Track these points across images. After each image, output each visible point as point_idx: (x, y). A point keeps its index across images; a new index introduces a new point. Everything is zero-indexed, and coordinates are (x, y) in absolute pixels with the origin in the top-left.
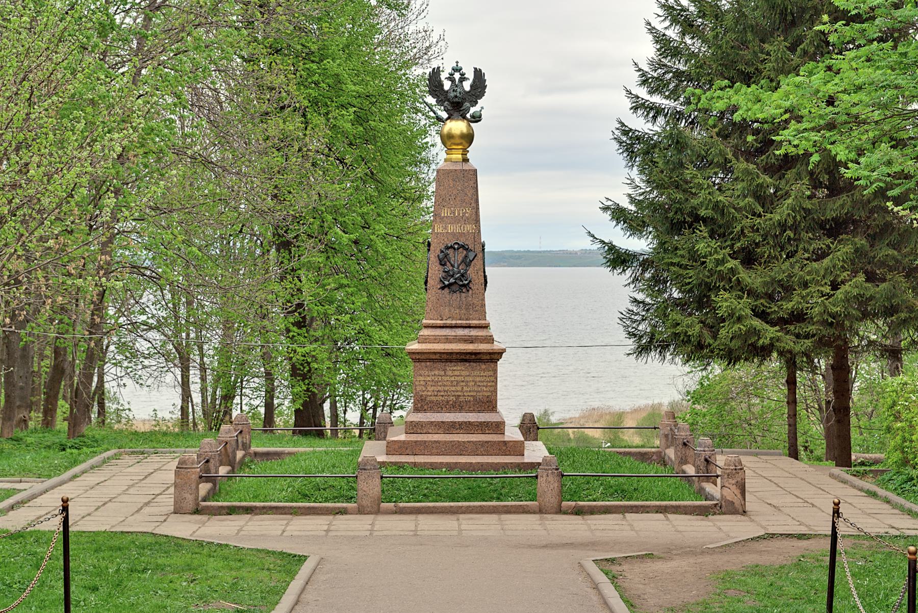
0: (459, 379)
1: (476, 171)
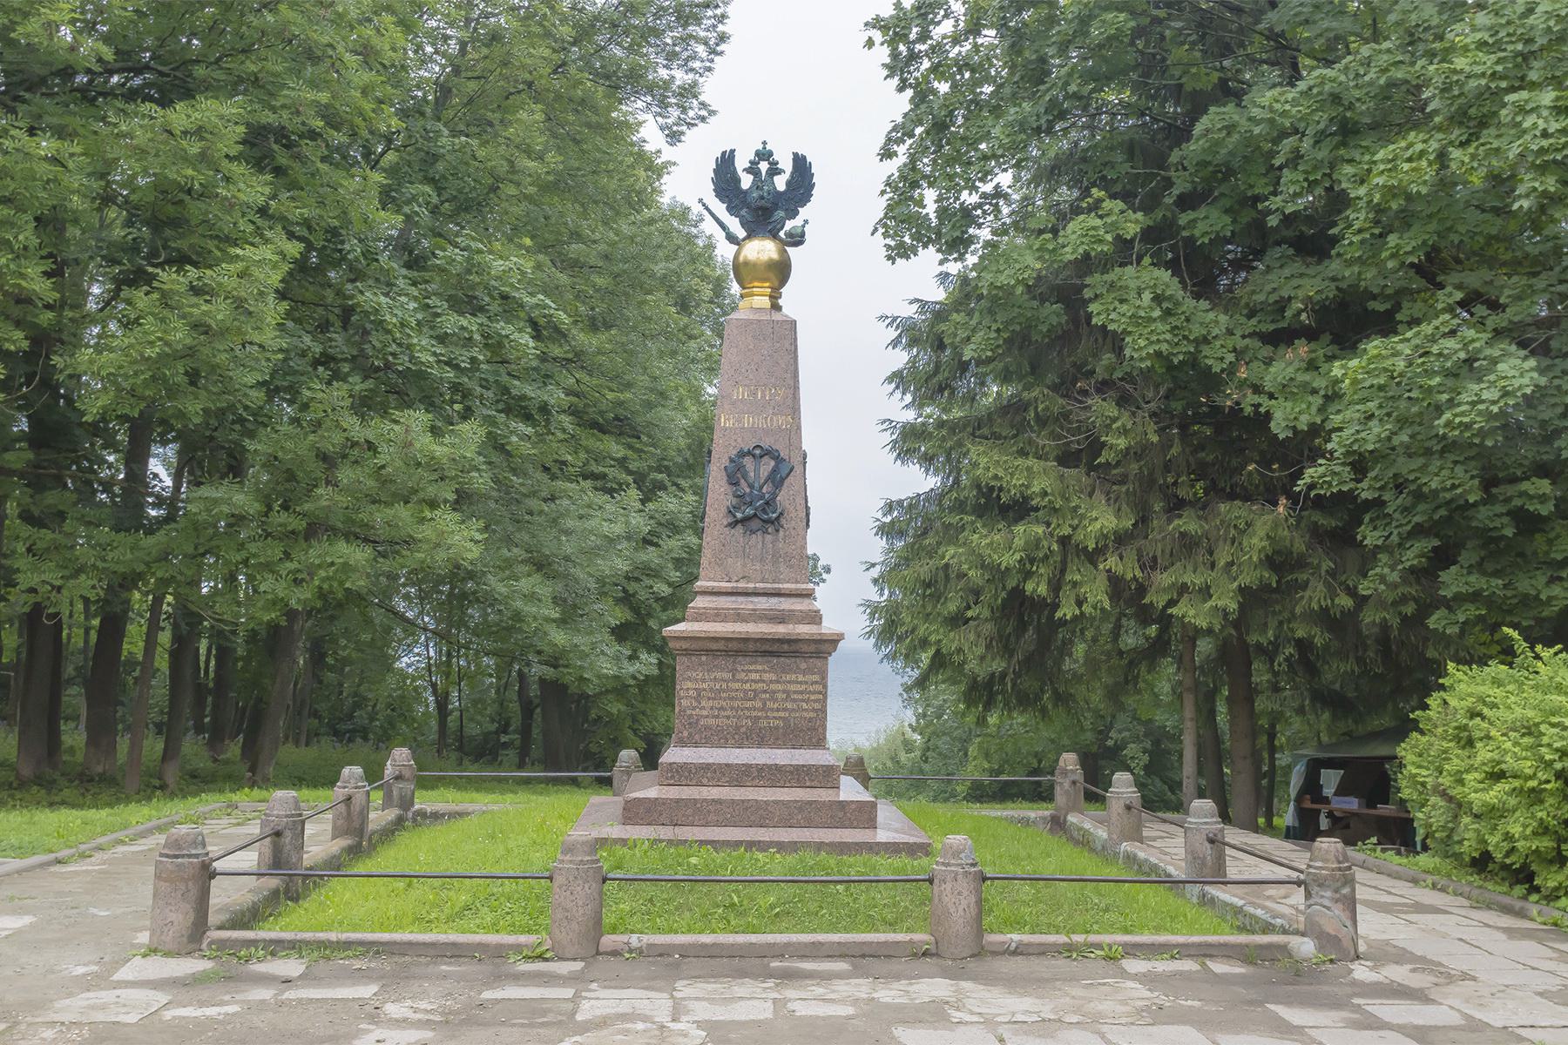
1: (794, 323)
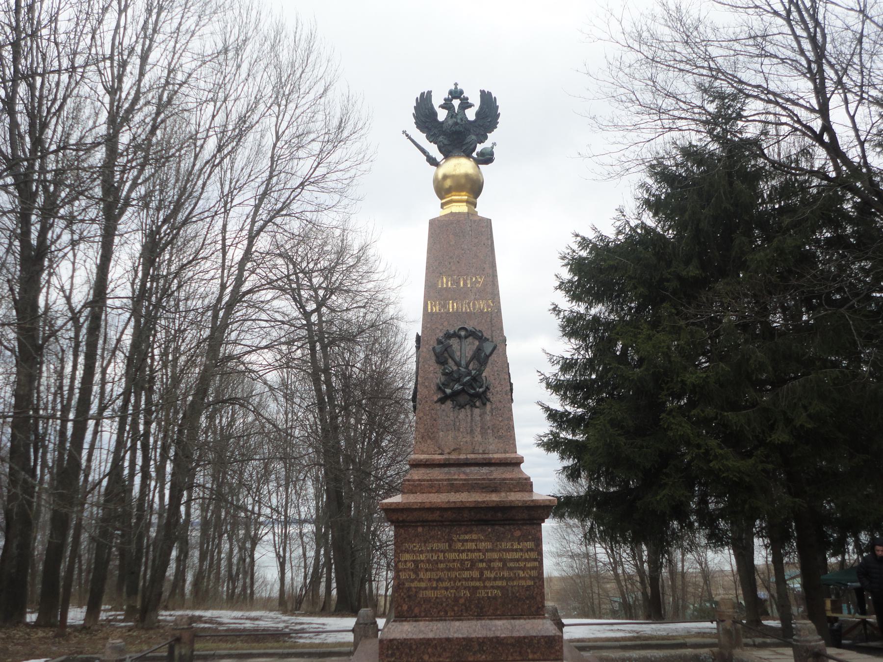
0: (475, 555)
